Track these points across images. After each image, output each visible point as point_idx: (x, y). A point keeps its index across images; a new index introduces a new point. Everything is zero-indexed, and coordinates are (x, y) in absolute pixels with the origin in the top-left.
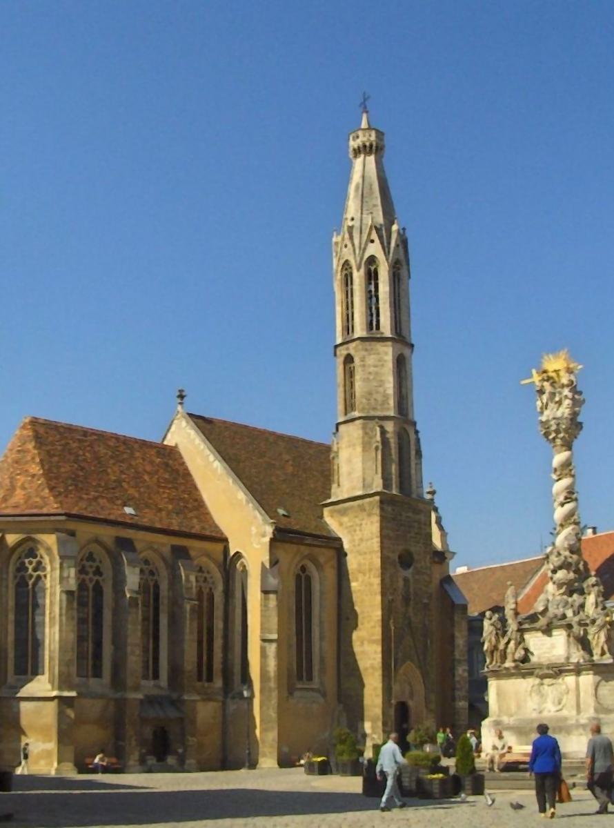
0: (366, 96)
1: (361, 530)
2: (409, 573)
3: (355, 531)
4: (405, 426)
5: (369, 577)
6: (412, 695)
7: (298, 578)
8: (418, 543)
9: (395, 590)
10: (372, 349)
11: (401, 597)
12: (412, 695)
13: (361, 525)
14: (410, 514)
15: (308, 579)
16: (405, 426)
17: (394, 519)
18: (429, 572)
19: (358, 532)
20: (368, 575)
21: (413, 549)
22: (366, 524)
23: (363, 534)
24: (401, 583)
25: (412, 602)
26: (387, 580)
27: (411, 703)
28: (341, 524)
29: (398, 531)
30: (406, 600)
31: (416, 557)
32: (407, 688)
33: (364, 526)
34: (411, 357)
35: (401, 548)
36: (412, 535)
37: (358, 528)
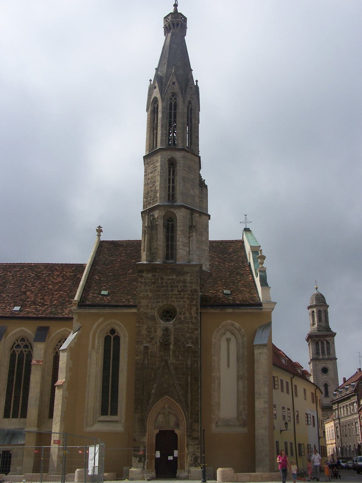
2: (170, 324)
4: (172, 210)
6: (177, 425)
7: (107, 340)
8: (184, 298)
9: (153, 338)
10: (150, 162)
11: (158, 344)
12: (177, 425)
14: (174, 277)
15: (117, 339)
16: (172, 210)
17: (154, 283)
18: (194, 320)
21: (175, 304)
24: (159, 333)
25: (172, 347)
26: (144, 332)
27: (177, 431)
30: (165, 345)
31: (178, 310)
32: (173, 420)
35: (161, 304)
36: (176, 292)
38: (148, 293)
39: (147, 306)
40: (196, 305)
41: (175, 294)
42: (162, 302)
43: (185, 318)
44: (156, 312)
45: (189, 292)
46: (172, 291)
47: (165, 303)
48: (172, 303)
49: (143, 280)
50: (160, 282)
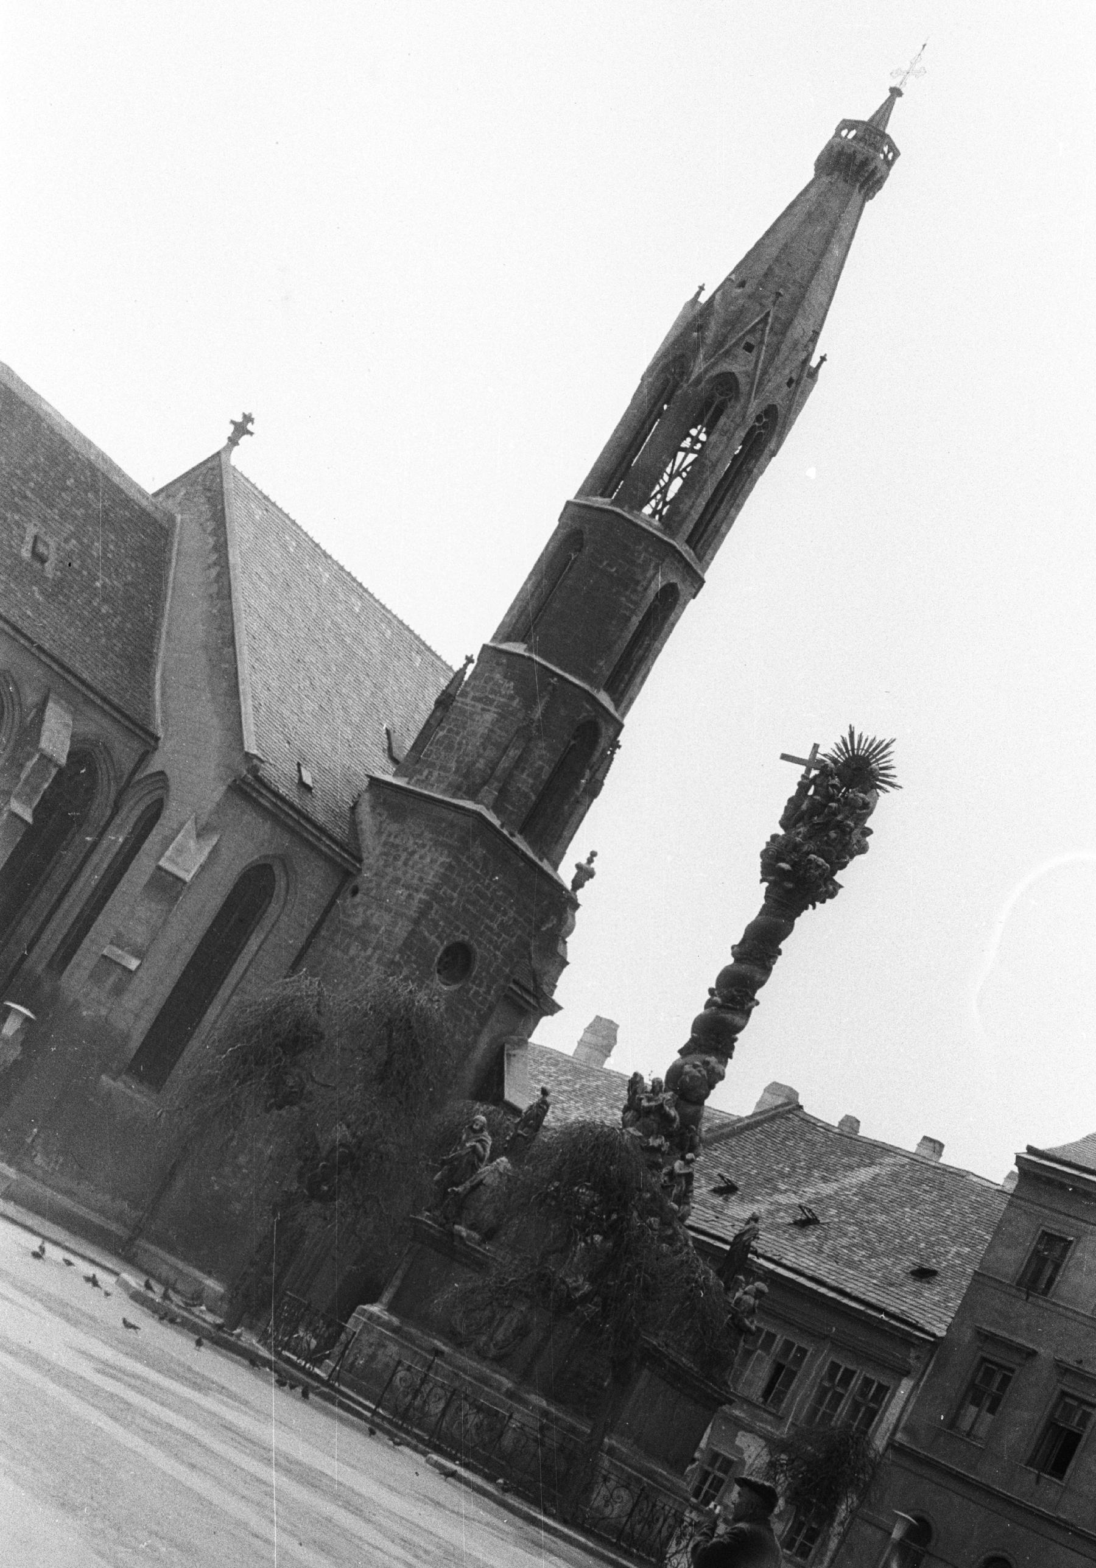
0: (917, 67)
1: (405, 864)
3: (396, 858)
5: (369, 958)
13: (413, 853)
19: (400, 863)
20: (369, 951)
21: (479, 951)
22: (421, 858)
23: (405, 873)
28: (379, 833)
29: (474, 903)
33: (416, 856)
34: (686, 603)
35: (460, 937)
37: (404, 856)
38: (455, 895)
39: (436, 925)
40: (507, 978)
41: (490, 928)
42: (464, 933)
43: (477, 993)
44: (442, 949)
45: (513, 940)
46: (492, 918)
47: (467, 937)
48: (475, 946)
49: (464, 860)
50: (486, 884)
